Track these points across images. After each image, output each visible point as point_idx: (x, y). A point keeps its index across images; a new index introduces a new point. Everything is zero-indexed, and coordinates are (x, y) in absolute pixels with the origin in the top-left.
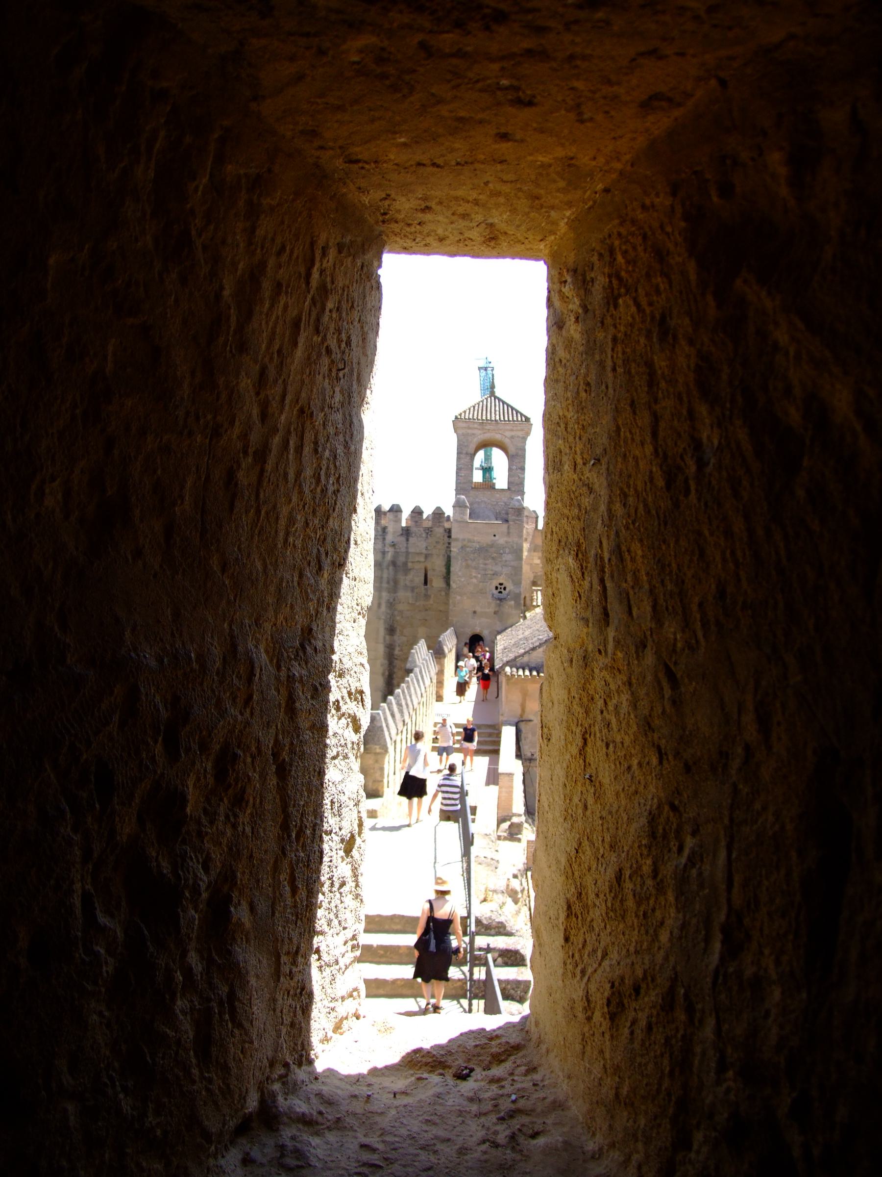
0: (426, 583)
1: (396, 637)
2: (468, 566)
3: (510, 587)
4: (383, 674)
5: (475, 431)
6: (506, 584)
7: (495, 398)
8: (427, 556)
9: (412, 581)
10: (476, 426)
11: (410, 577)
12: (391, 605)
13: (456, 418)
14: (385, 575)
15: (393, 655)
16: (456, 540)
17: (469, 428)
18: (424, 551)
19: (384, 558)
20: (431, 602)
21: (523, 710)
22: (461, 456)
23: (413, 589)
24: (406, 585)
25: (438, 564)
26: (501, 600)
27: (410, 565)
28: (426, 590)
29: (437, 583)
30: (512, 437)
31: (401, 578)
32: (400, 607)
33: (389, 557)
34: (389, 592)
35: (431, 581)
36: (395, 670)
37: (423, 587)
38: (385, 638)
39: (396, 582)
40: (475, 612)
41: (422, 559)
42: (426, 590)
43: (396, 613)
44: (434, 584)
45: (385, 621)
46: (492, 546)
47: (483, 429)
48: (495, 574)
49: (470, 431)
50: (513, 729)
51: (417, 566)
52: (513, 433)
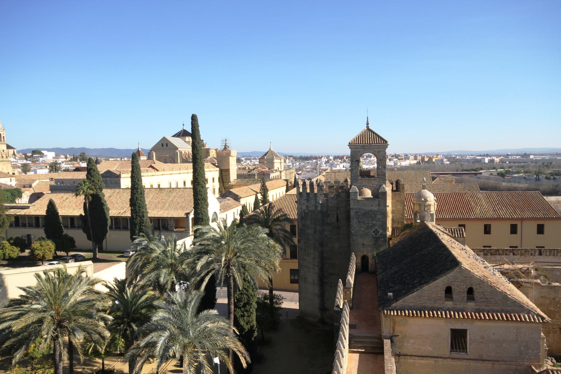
0: (337, 221)
2: (359, 222)
3: (381, 231)
5: (360, 150)
6: (378, 230)
13: (349, 143)
16: (353, 209)
17: (356, 148)
21: (394, 330)
22: (354, 163)
26: (376, 238)
27: (329, 212)
33: (319, 209)
40: (363, 244)
46: (371, 211)
48: (373, 225)
49: (357, 150)
50: (389, 341)
52: (379, 150)
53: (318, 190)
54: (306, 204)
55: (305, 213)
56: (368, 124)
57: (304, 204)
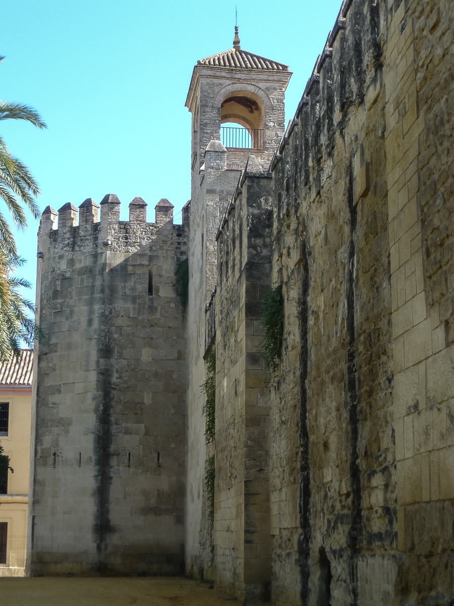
1: (113, 361)
4: (96, 410)
7: (241, 52)
8: (151, 258)
9: (133, 289)
10: (224, 74)
11: (130, 284)
12: (106, 319)
14: (98, 283)
15: (109, 383)
18: (148, 252)
19: (95, 262)
20: (158, 315)
23: (134, 299)
24: (125, 295)
25: (167, 268)
27: (130, 269)
28: (151, 300)
29: (166, 292)
30: (268, 89)
31: (119, 284)
32: (119, 322)
34: (104, 303)
35: (158, 290)
36: (113, 404)
37: (147, 297)
38: (98, 362)
39: (113, 290)
41: (146, 263)
42: (151, 300)
43: (113, 329)
44: (162, 293)
45: (99, 340)
47: (232, 78)
49: (216, 81)
51: (139, 271)
53: (103, 214)
54: (68, 255)
55: (64, 279)
56: (236, 43)
57: (61, 257)
